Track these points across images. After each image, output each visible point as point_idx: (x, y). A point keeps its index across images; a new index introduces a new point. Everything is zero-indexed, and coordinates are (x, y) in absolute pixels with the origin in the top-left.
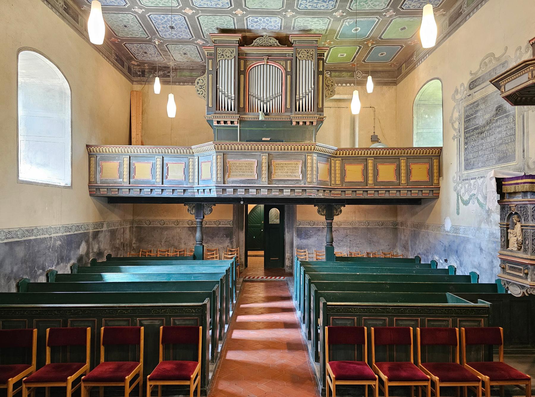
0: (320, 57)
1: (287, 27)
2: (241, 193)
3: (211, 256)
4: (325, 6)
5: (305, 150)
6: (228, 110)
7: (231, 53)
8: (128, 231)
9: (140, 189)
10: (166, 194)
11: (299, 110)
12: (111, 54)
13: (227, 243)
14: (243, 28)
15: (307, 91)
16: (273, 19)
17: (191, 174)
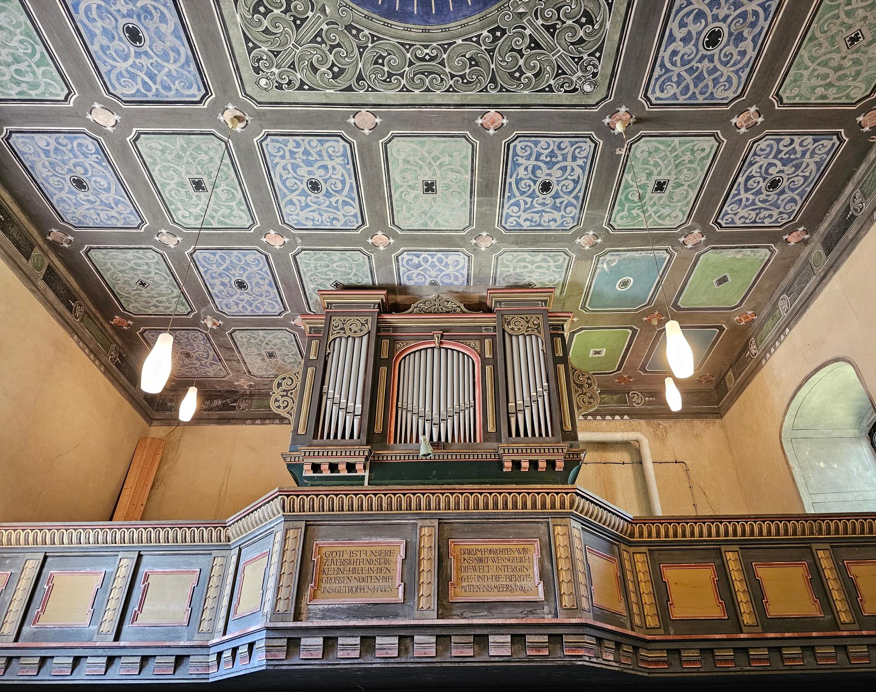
4: (559, 222)
5: (544, 506)
12: (107, 349)
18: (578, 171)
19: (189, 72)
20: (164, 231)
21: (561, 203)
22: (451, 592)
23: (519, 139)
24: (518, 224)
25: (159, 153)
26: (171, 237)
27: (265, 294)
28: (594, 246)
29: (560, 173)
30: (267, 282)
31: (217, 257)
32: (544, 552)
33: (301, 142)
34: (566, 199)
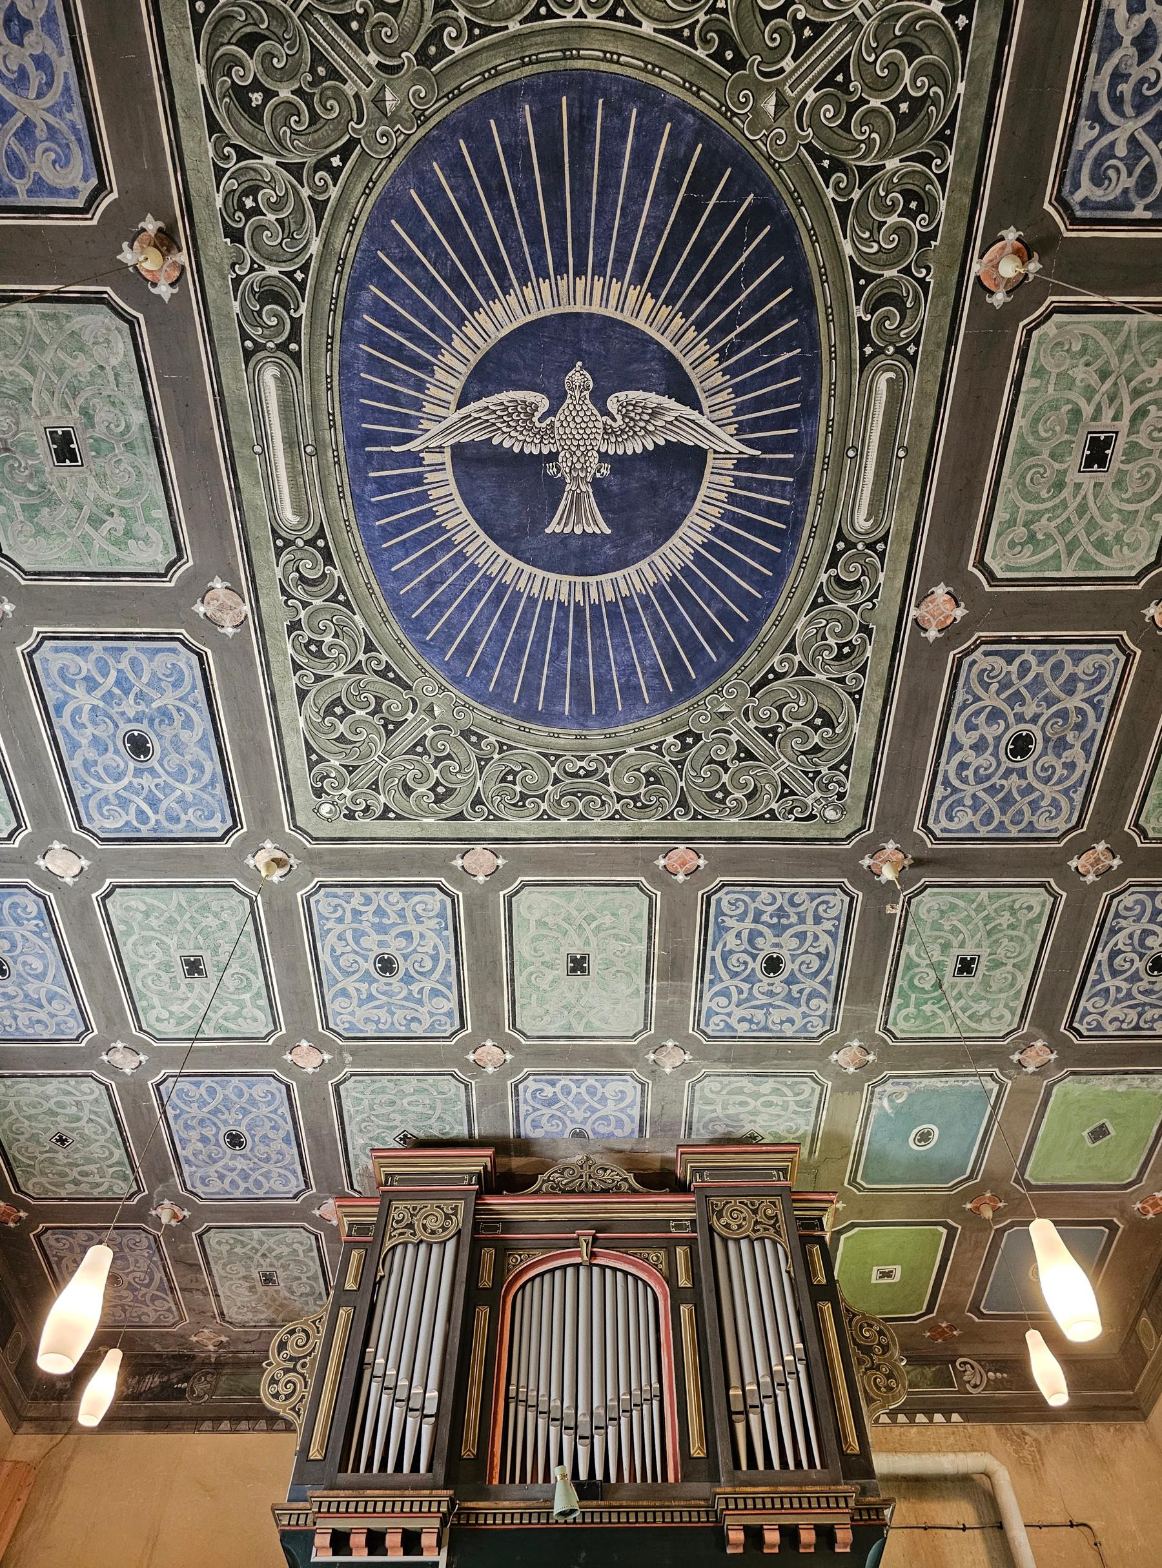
0: (808, 1237)
1: (664, 1128)
7: (447, 1217)
16: (614, 1086)
18: (826, 940)
19: (213, 796)
20: (120, 1045)
21: (801, 992)
23: (726, 889)
24: (729, 1026)
25: (139, 916)
26: (129, 1054)
27: (274, 1157)
28: (862, 1066)
29: (795, 942)
30: (282, 1134)
31: (203, 1090)
33: (373, 896)
34: (809, 985)
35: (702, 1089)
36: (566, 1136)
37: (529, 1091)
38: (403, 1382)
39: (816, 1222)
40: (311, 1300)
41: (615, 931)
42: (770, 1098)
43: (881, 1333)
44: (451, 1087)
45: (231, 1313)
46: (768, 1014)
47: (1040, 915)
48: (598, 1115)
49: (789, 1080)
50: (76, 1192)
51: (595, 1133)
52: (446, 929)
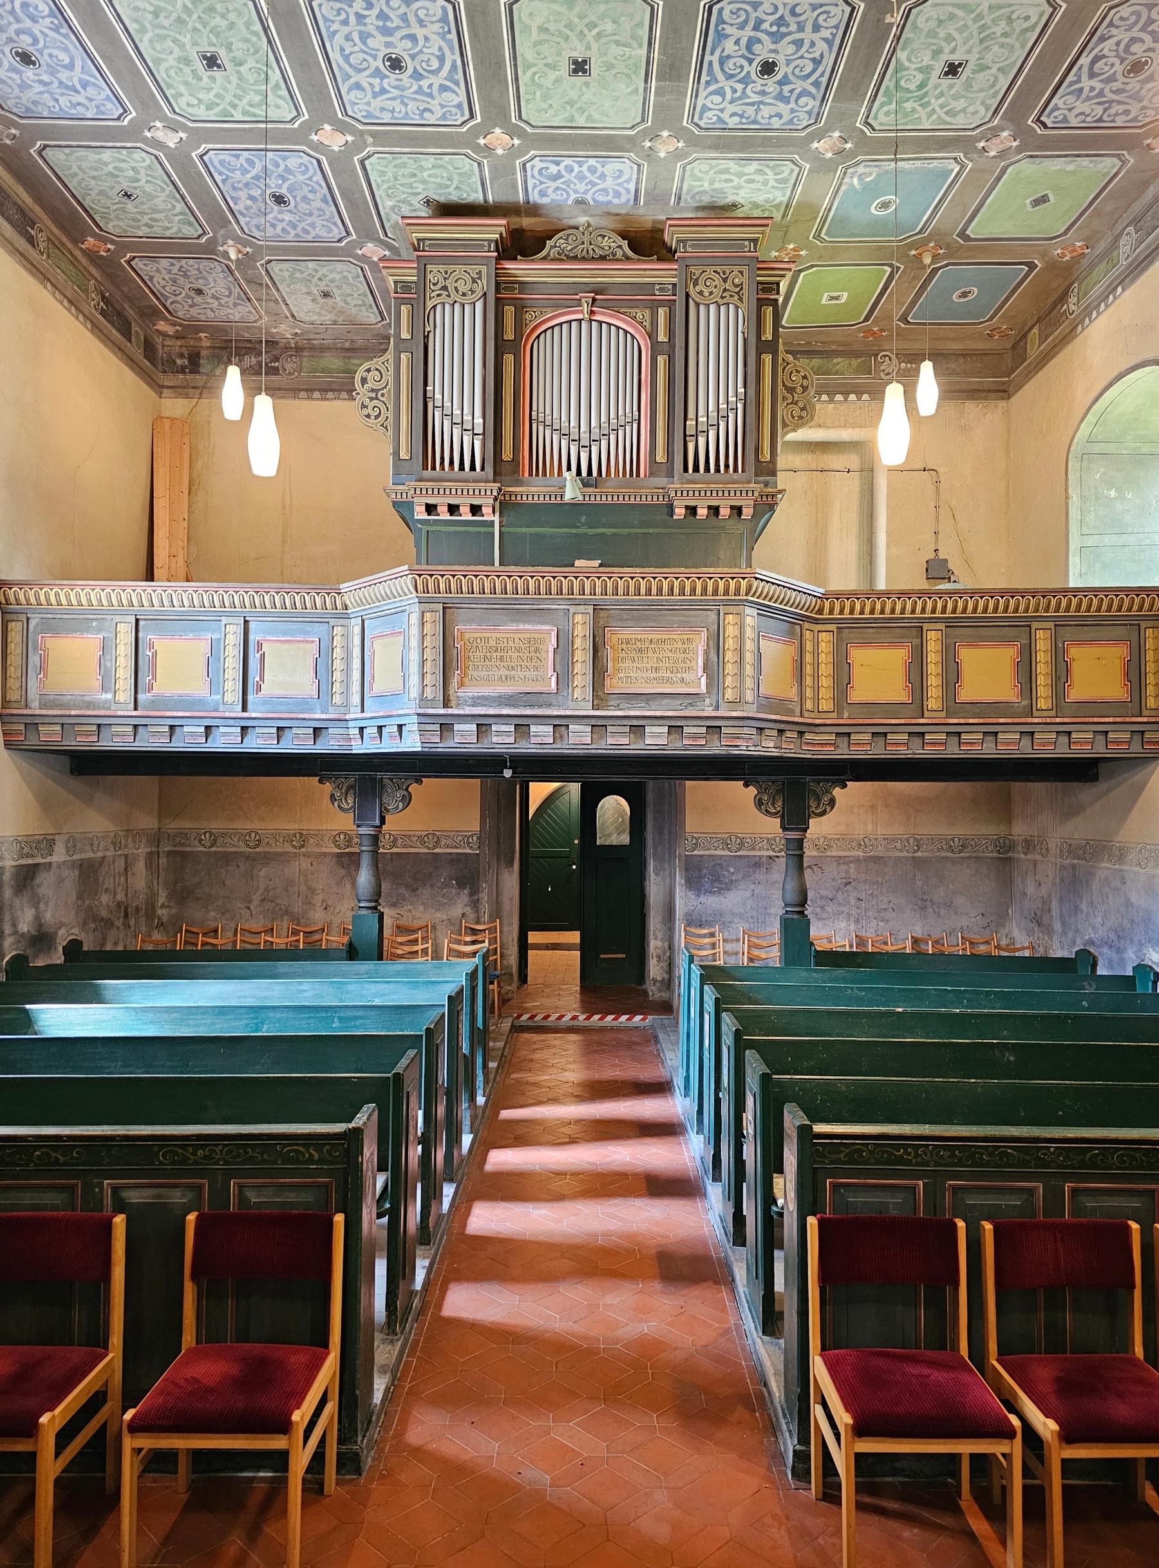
0: (766, 296)
2: (502, 740)
3: (407, 949)
5: (716, 593)
6: (462, 468)
7: (474, 281)
8: (140, 866)
9: (172, 727)
10: (258, 743)
11: (696, 469)
12: (86, 291)
13: (460, 906)
14: (511, 199)
15: (723, 406)
16: (612, 166)
17: (337, 676)
18: (822, 46)
20: (158, 124)
21: (791, 91)
22: (607, 682)
24: (720, 120)
25: (150, 17)
26: (170, 134)
27: (316, 213)
28: (840, 152)
29: (791, 49)
31: (242, 160)
32: (711, 643)
34: (799, 86)
35: (692, 169)
36: (570, 202)
37: (536, 170)
38: (457, 412)
39: (775, 286)
40: (363, 309)
41: (617, 37)
42: (752, 177)
43: (804, 377)
44: (465, 164)
45: (301, 315)
46: (758, 110)
47: (1036, 24)
48: (597, 188)
49: (772, 163)
50: (100, 153)
51: (594, 199)
52: (449, 32)
